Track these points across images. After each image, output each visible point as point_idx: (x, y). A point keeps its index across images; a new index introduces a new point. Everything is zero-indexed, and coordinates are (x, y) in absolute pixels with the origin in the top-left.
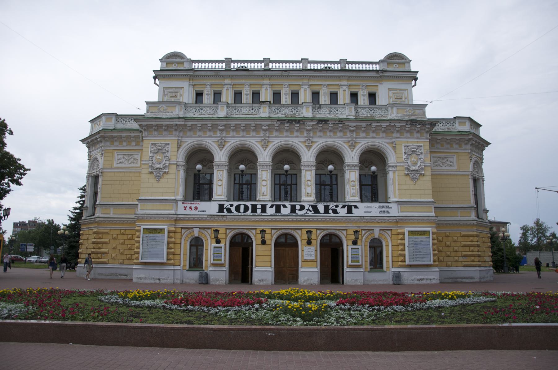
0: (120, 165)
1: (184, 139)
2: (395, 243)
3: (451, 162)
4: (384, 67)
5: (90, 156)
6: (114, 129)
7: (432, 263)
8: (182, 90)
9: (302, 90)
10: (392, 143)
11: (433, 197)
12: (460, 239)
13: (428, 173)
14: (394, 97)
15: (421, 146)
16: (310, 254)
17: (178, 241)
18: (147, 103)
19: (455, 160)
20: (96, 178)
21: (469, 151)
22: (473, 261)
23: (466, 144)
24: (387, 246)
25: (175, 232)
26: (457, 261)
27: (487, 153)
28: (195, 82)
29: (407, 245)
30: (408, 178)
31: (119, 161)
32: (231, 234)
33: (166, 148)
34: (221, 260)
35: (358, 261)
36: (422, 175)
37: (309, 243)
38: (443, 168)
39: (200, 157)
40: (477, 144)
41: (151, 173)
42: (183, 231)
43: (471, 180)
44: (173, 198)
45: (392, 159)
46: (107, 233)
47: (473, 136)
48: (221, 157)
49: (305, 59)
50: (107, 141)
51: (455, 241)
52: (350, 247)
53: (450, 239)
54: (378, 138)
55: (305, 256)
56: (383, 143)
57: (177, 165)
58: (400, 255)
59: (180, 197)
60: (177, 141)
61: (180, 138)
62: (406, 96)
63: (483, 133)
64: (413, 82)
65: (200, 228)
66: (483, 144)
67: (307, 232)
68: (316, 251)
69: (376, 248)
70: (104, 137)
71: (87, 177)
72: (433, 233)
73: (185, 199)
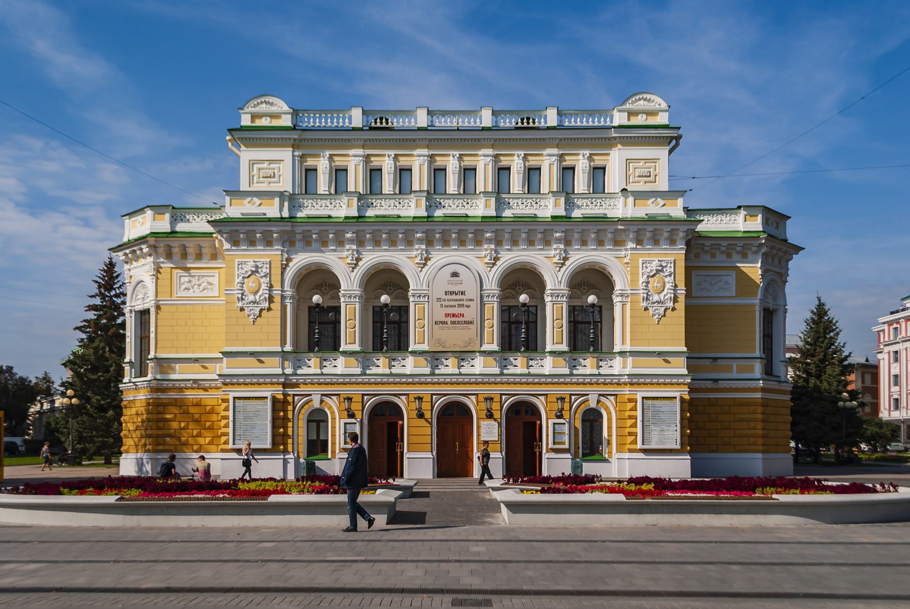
16: (491, 433)
24: (610, 419)
27: (795, 264)
37: (490, 416)
38: (713, 293)
40: (775, 252)
52: (551, 422)
55: (482, 435)
60: (279, 258)
64: (674, 142)
67: (486, 399)
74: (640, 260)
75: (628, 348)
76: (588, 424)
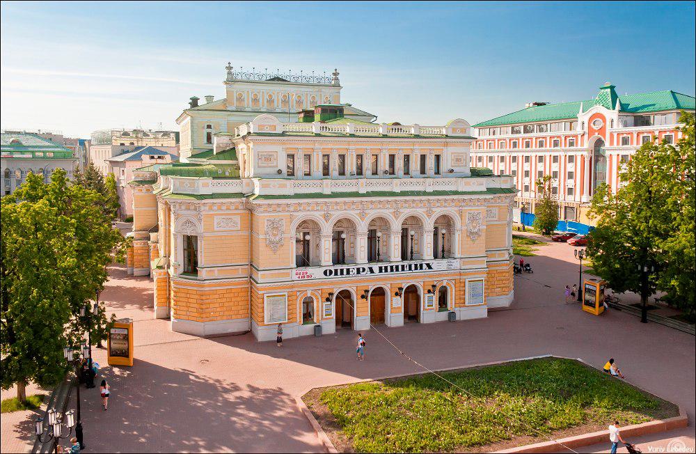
1: (295, 214)
12: (497, 275)
13: (483, 234)
24: (452, 291)
29: (467, 291)
34: (331, 315)
36: (479, 236)
42: (298, 293)
45: (458, 224)
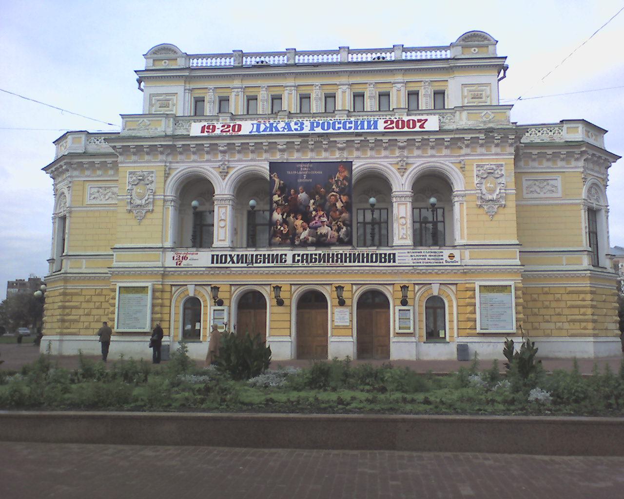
0: (94, 202)
1: (174, 165)
2: (462, 302)
3: (553, 186)
4: (457, 52)
5: (56, 190)
6: (84, 153)
7: (514, 331)
8: (175, 98)
9: (340, 91)
10: (460, 162)
11: (519, 237)
12: (565, 297)
13: (512, 204)
14: (470, 96)
15: (502, 165)
17: (167, 302)
18: (123, 116)
19: (559, 183)
20: (64, 218)
21: (582, 170)
22: (585, 329)
23: (577, 159)
24: (451, 306)
25: (162, 291)
26: (560, 329)
27: (615, 171)
28: (192, 86)
30: (481, 211)
31: (93, 196)
32: (237, 293)
33: (149, 178)
35: (409, 328)
37: (342, 303)
38: (542, 195)
39: (195, 189)
41: (130, 211)
43: (583, 211)
44: (160, 245)
45: (458, 185)
46: (76, 294)
47: (587, 147)
48: (223, 188)
49: (344, 48)
50: (75, 169)
51: (558, 300)
52: (397, 308)
53: (551, 297)
54: (440, 157)
56: (447, 163)
57: (165, 201)
58: (469, 320)
59: (168, 244)
60: (163, 169)
61: (168, 164)
62: (488, 93)
63: (609, 143)
65: (196, 285)
66: (605, 159)
68: (351, 313)
69: (435, 308)
70: (70, 164)
71: (53, 218)
72: (516, 289)
73: (179, 244)
74: (475, 164)
75: (464, 242)
76: (431, 311)
